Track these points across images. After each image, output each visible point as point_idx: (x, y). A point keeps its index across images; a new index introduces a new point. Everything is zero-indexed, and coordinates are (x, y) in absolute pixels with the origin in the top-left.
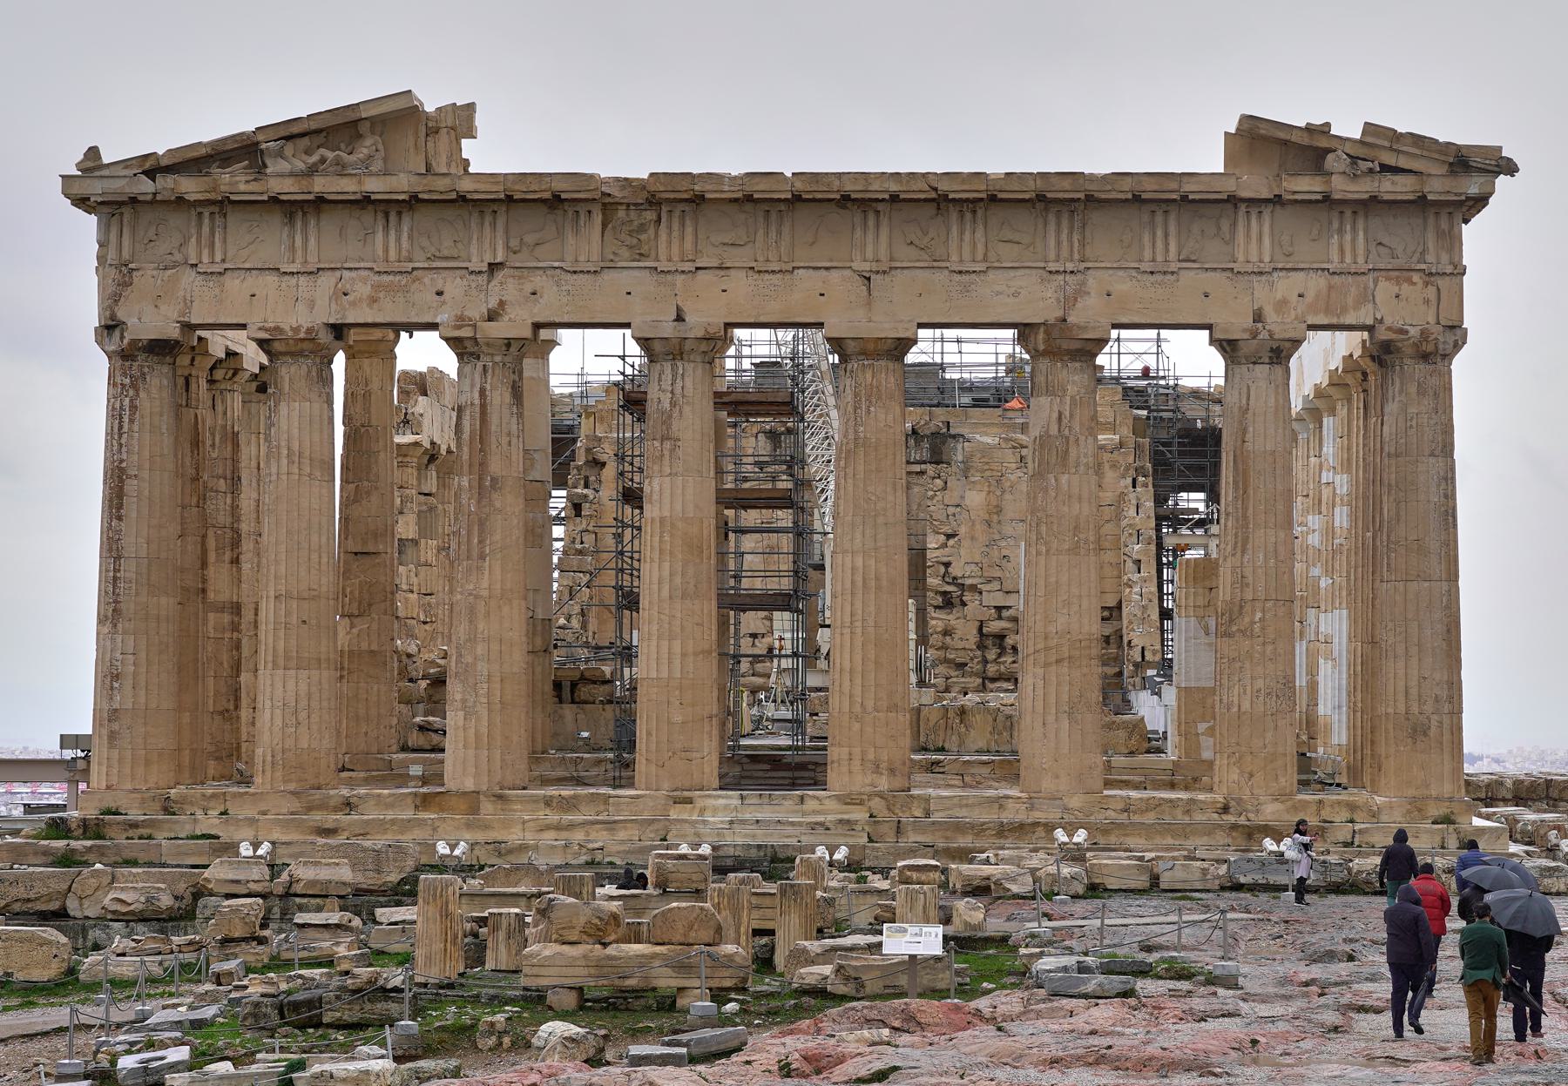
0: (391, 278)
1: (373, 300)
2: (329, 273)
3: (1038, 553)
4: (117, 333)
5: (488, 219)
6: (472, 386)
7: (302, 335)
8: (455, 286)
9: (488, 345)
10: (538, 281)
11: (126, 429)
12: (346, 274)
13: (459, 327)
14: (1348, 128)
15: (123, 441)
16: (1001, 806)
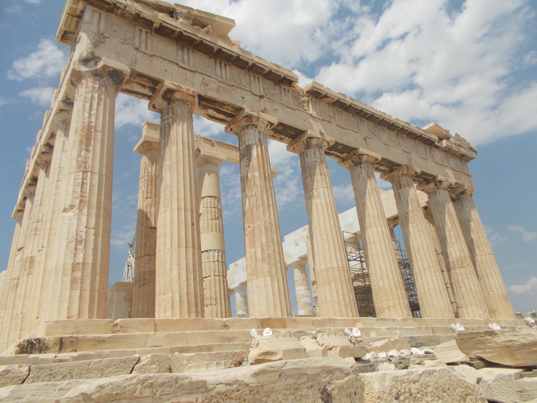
0: (224, 85)
1: (218, 91)
2: (200, 74)
3: (420, 235)
4: (92, 63)
5: (257, 79)
6: (255, 138)
7: (190, 93)
8: (249, 98)
9: (262, 122)
10: (276, 106)
11: (95, 106)
12: (206, 77)
13: (253, 111)
14: (452, 133)
15: (94, 112)
16: (443, 323)
